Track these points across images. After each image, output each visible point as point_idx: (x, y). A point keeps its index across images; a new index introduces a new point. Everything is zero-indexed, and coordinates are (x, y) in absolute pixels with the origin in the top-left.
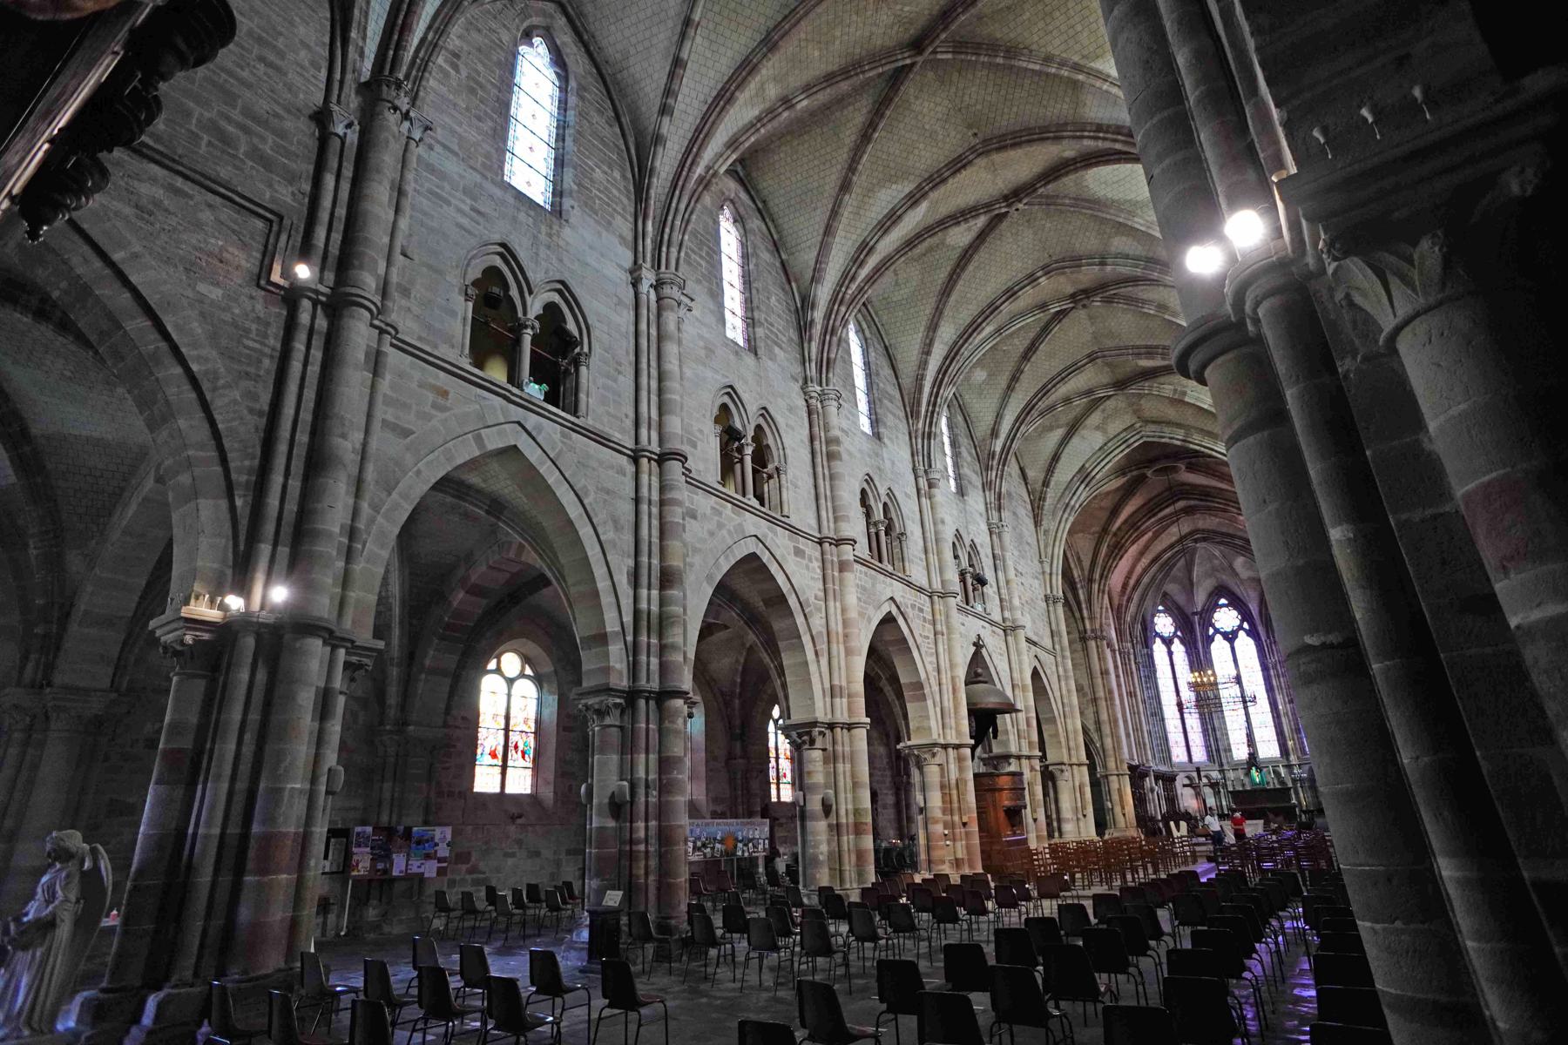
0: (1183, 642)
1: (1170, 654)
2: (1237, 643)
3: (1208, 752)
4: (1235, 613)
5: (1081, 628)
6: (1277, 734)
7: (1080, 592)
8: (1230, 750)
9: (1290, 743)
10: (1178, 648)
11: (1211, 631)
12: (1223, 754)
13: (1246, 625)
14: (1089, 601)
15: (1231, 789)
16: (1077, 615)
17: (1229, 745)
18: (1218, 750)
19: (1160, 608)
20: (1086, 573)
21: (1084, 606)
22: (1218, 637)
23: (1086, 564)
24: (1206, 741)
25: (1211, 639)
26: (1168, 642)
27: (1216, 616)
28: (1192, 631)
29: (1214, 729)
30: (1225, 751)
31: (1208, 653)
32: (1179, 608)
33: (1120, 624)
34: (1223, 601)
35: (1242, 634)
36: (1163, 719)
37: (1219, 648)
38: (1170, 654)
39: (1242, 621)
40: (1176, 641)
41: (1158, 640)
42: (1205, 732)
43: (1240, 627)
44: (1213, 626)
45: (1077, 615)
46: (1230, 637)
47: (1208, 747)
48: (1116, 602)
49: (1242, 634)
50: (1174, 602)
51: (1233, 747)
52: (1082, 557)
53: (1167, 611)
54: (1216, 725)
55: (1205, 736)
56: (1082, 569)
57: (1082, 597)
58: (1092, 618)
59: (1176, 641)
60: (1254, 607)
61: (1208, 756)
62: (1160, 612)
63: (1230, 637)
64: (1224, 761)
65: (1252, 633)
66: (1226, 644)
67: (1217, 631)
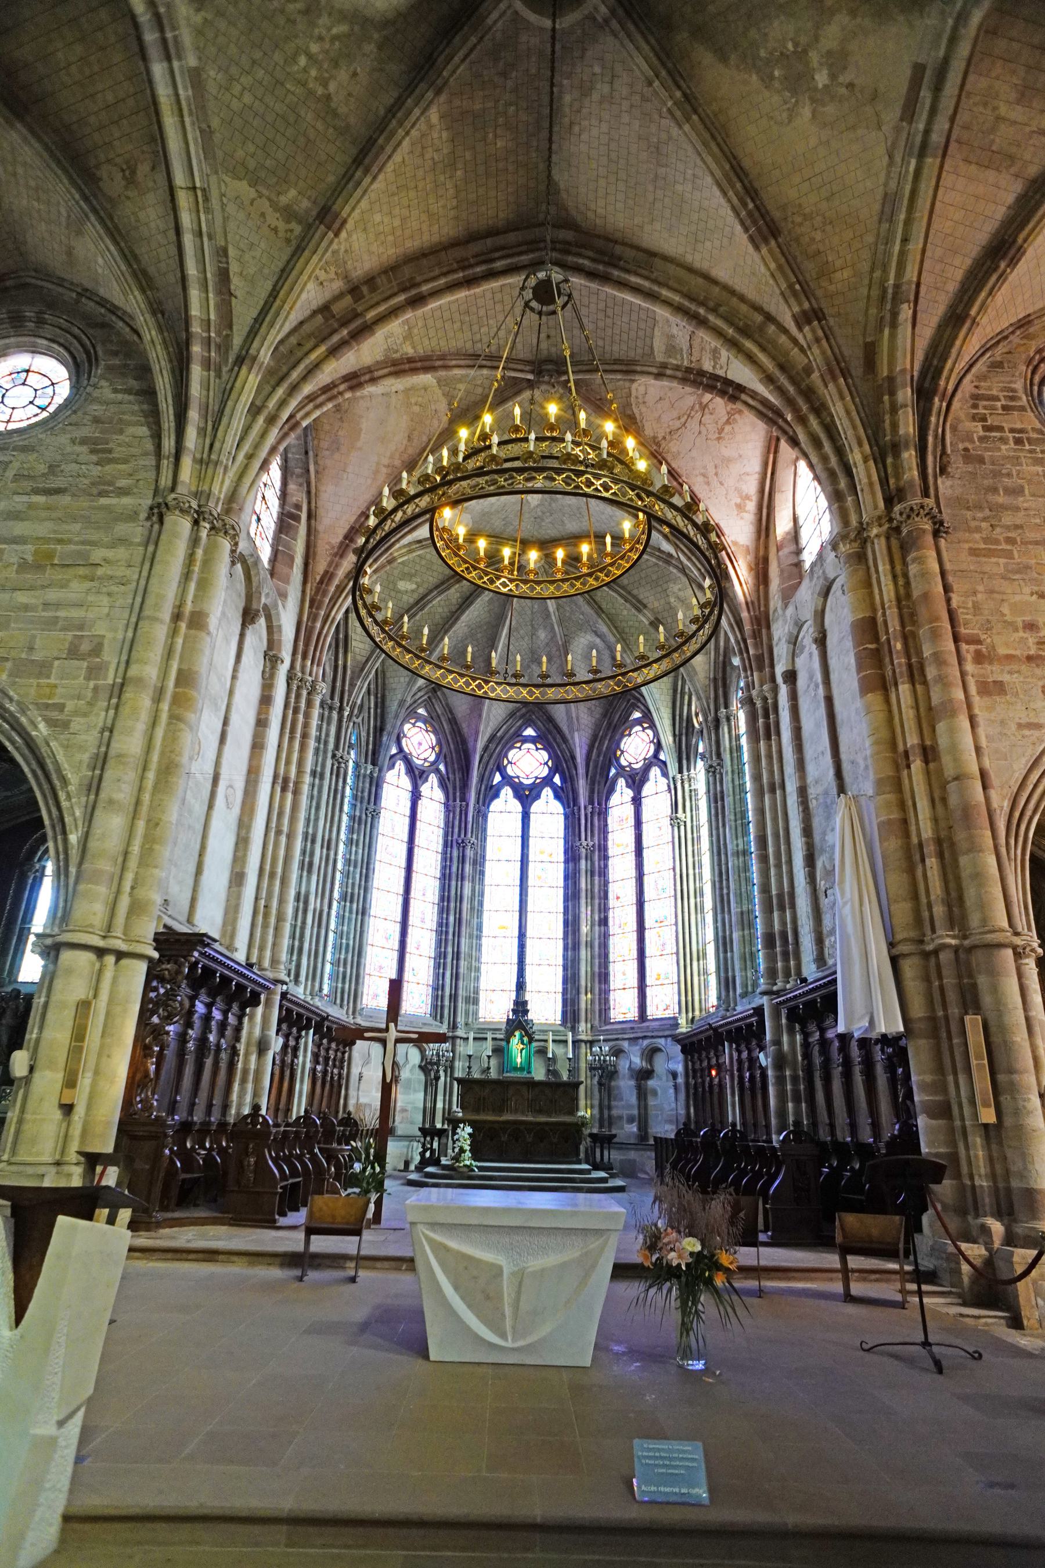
0: (443, 784)
1: (416, 797)
2: (536, 807)
3: (435, 998)
4: (544, 755)
5: (165, 481)
6: (565, 981)
7: (196, 371)
8: (476, 1002)
9: (584, 999)
10: (432, 792)
11: (497, 778)
12: (461, 1005)
13: (557, 779)
14: (215, 419)
15: (459, 1074)
16: (168, 444)
17: (476, 991)
18: (454, 998)
19: (421, 711)
20: (237, 341)
21: (193, 415)
22: (507, 792)
23: (244, 314)
24: (436, 976)
25: (491, 793)
26: (417, 775)
27: (513, 754)
28: (465, 769)
29: (457, 956)
30: (467, 1000)
31: (482, 815)
32: (453, 721)
33: (313, 617)
34: (530, 732)
35: (547, 793)
36: (364, 912)
37: (505, 807)
38: (416, 797)
39: (553, 771)
40: (433, 779)
41: (400, 766)
42: (440, 958)
43: (547, 781)
44: (501, 769)
45: (168, 444)
46: (526, 795)
47: (438, 988)
48: (320, 567)
49: (547, 793)
50: (449, 709)
51: (482, 996)
52: (236, 283)
53: (433, 722)
54: (464, 948)
55: (437, 966)
56: (227, 320)
57: (195, 390)
58: (206, 463)
59: (433, 779)
60: (579, 744)
61: (434, 1007)
62: (419, 718)
63: (526, 795)
64: (460, 1020)
65: (566, 796)
66: (516, 806)
67: (507, 780)
